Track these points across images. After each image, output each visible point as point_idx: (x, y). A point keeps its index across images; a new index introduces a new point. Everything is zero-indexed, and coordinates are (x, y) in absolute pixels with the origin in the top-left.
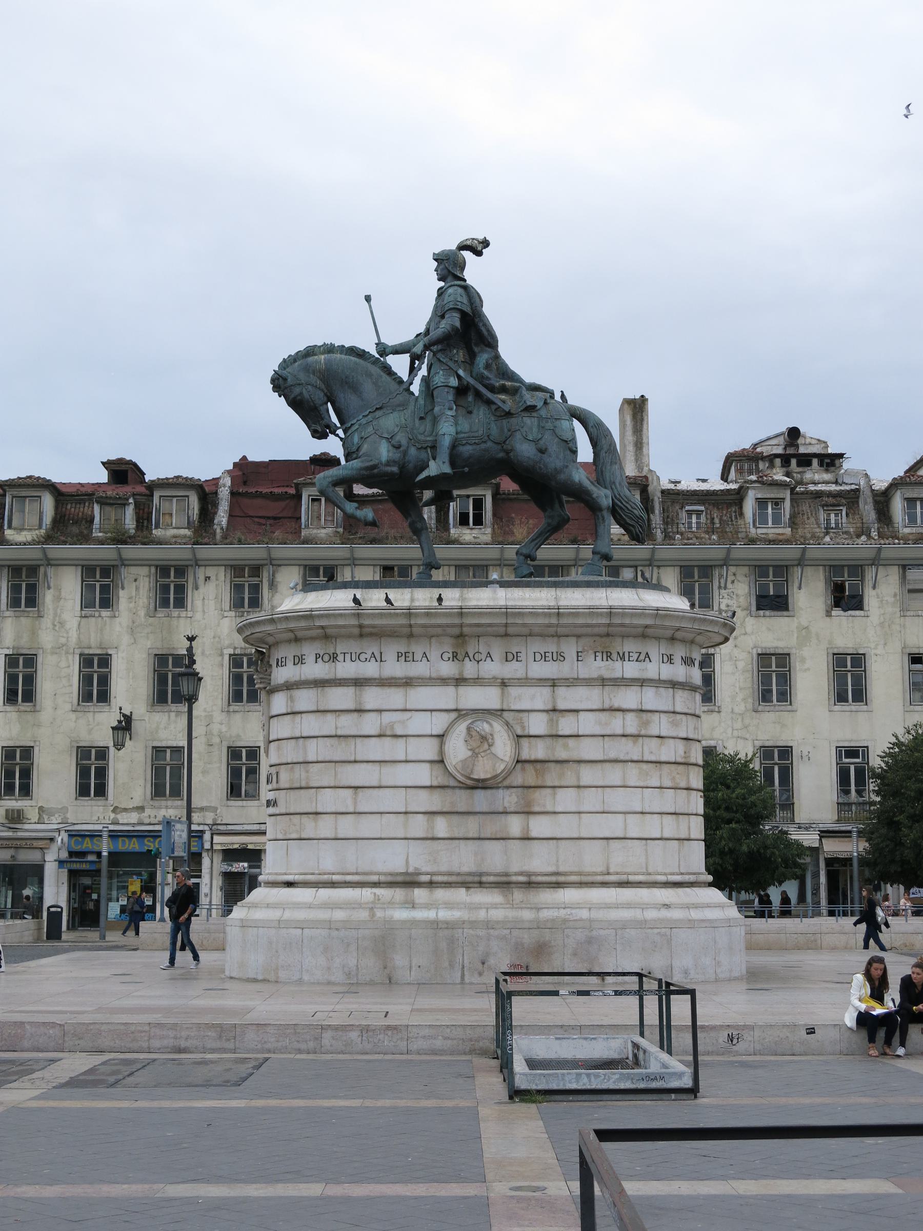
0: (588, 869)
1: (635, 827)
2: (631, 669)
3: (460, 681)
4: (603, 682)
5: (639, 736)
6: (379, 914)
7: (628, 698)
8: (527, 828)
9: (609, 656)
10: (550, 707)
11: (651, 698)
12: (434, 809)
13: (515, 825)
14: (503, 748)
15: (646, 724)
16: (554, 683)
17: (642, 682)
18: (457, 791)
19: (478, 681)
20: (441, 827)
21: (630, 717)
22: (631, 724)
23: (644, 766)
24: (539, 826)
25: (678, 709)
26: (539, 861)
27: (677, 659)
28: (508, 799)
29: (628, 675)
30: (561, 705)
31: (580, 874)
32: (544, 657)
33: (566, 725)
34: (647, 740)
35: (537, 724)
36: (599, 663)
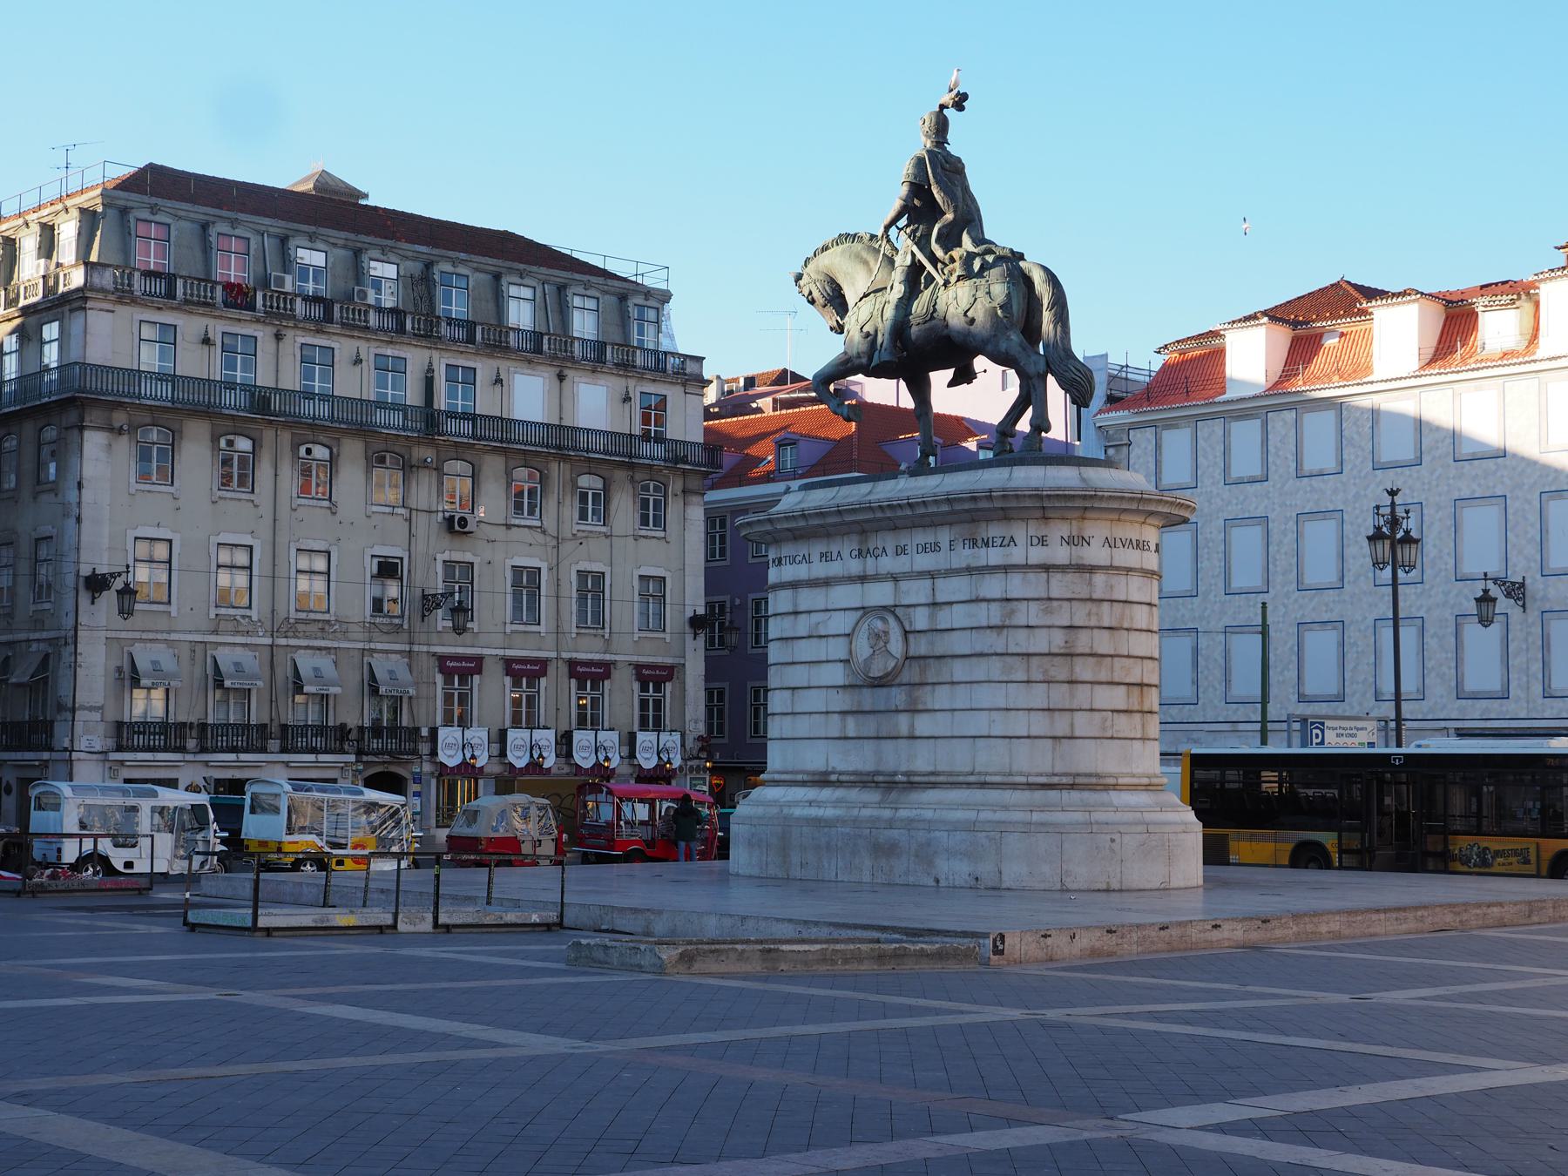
0: (958, 769)
1: (1000, 726)
2: (994, 556)
3: (863, 579)
4: (970, 570)
5: (1003, 627)
6: (786, 811)
7: (993, 586)
8: (912, 726)
9: (974, 543)
10: (930, 600)
11: (1016, 585)
12: (845, 708)
13: (903, 723)
14: (896, 646)
15: (1013, 612)
16: (932, 575)
17: (1006, 569)
18: (865, 690)
19: (877, 578)
20: (851, 727)
21: (994, 606)
22: (994, 614)
23: (1008, 659)
24: (924, 725)
25: (1053, 595)
26: (922, 760)
27: (815, 557)
28: (898, 697)
29: (992, 562)
30: (940, 599)
31: (951, 774)
32: (925, 549)
33: (945, 618)
34: (1012, 631)
35: (921, 620)
36: (967, 552)
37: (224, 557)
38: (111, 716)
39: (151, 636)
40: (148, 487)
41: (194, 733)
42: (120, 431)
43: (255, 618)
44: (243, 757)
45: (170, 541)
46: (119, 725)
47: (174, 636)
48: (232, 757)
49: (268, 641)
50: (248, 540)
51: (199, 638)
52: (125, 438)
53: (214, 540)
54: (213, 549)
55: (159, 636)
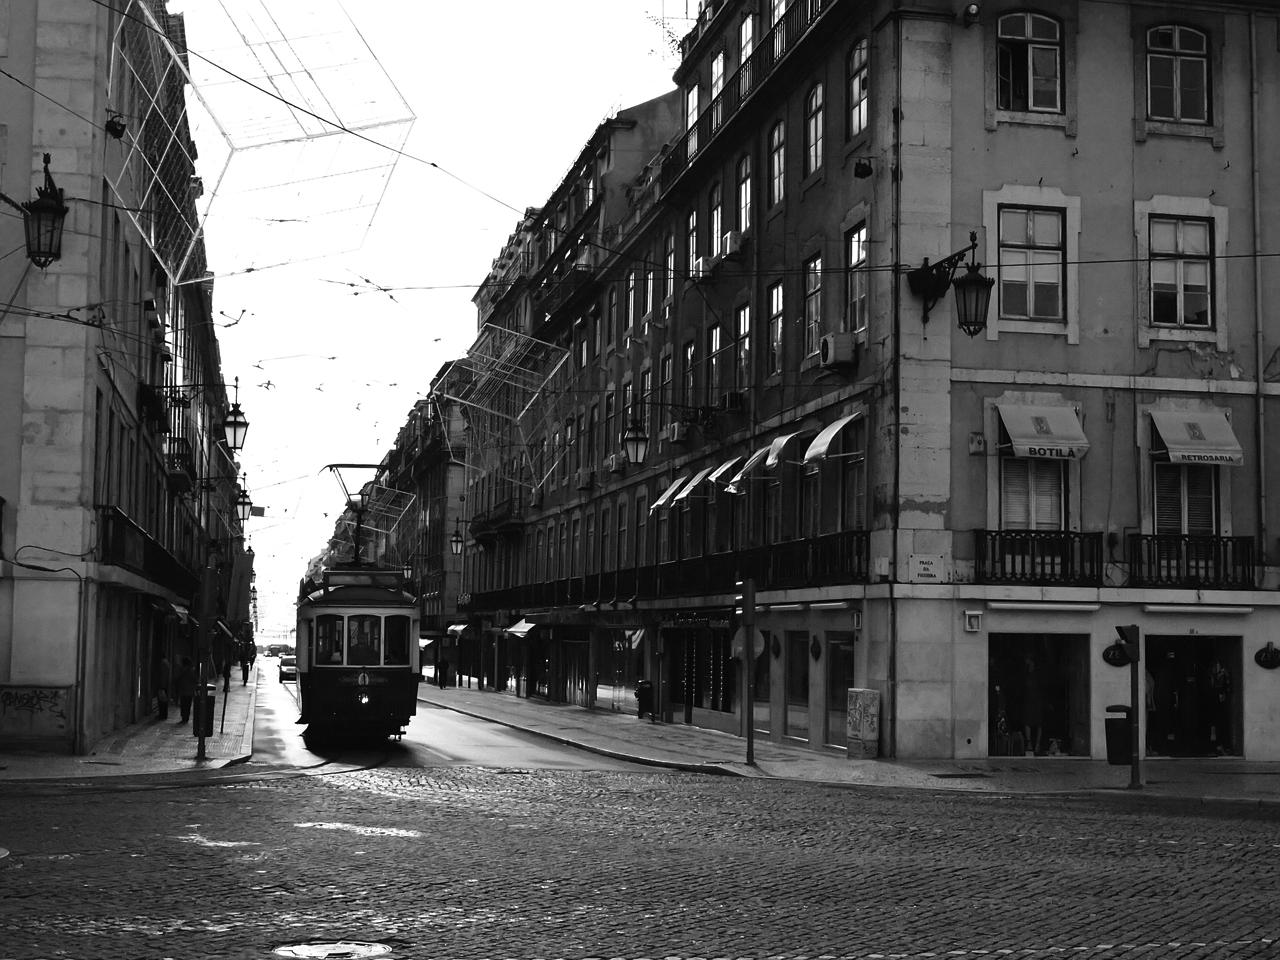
37: (1163, 238)
38: (965, 520)
39: (1033, 378)
40: (1019, 116)
41: (1118, 553)
42: (967, 21)
43: (1223, 346)
44: (1210, 596)
45: (1062, 212)
46: (980, 535)
47: (1076, 379)
48: (1189, 596)
49: (1247, 387)
50: (1200, 207)
51: (1120, 382)
52: (976, 32)
53: (1142, 208)
54: (1142, 224)
55: (1048, 379)
